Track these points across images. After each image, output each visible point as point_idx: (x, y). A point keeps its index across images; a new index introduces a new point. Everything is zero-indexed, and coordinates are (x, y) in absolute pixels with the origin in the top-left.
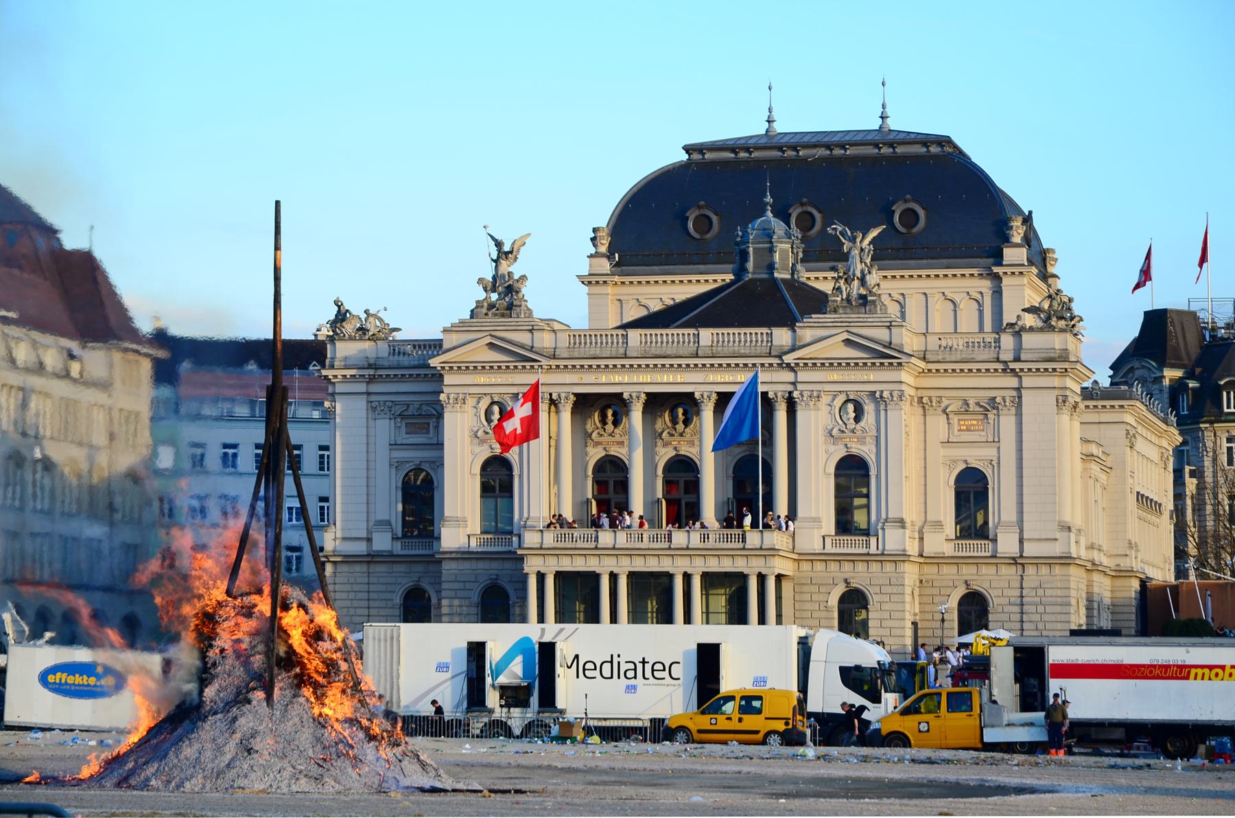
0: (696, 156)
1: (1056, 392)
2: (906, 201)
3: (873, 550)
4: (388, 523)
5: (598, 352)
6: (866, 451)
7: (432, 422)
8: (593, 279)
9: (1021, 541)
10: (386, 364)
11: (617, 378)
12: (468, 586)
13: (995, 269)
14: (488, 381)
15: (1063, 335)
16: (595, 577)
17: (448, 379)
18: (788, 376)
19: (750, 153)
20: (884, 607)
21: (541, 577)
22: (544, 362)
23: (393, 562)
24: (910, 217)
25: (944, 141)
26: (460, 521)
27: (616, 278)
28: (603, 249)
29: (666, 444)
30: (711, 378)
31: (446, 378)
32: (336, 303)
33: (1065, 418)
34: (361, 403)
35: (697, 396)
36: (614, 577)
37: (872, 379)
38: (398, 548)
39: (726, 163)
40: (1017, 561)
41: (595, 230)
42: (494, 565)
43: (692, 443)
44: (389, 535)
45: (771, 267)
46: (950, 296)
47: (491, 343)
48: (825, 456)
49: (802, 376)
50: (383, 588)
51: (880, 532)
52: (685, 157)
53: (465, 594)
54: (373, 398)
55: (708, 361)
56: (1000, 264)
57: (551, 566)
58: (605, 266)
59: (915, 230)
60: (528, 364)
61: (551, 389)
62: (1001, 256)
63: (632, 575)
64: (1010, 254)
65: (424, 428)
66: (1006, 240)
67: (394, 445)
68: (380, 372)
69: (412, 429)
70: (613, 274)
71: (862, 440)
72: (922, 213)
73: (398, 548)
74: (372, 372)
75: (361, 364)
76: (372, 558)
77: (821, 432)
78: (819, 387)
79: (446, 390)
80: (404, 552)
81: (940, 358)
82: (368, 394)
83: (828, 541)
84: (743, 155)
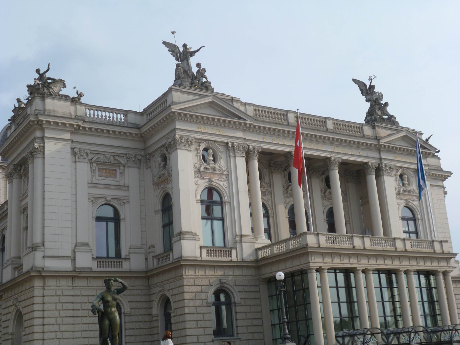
4: (86, 245)
23: (93, 277)
26: (194, 236)
32: (38, 71)
38: (94, 266)
44: (90, 254)
47: (212, 102)
49: (384, 156)
53: (203, 296)
54: (74, 145)
61: (249, 143)
67: (91, 184)
73: (94, 266)
76: (76, 275)
80: (99, 270)
82: (72, 141)
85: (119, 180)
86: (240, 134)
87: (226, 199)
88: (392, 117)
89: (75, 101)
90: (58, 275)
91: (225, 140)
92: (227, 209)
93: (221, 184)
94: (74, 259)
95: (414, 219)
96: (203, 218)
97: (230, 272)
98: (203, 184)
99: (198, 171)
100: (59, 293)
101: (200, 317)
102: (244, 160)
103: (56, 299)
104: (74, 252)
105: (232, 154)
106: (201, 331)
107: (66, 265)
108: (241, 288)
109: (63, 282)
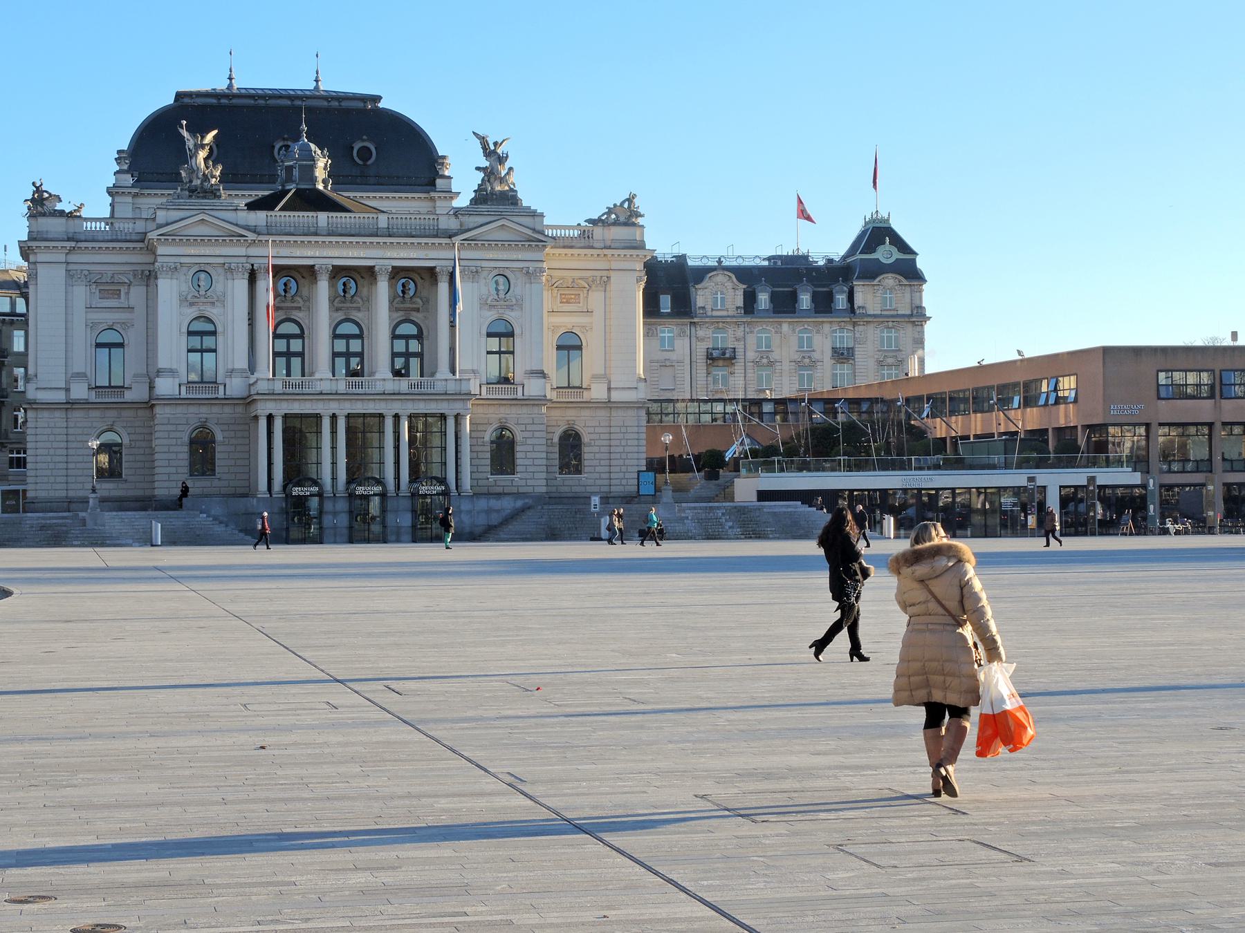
0: (187, 100)
2: (364, 141)
3: (520, 395)
4: (84, 375)
5: (292, 230)
6: (511, 316)
7: (123, 290)
8: (121, 190)
9: (609, 389)
10: (83, 238)
11: (310, 253)
12: (180, 428)
13: (433, 194)
14: (197, 253)
16: (318, 417)
17: (161, 250)
20: (529, 442)
21: (270, 418)
22: (251, 236)
25: (378, 99)
26: (172, 372)
27: (136, 190)
28: (125, 167)
29: (338, 310)
30: (389, 255)
34: (61, 271)
35: (377, 269)
36: (334, 417)
37: (520, 257)
38: (93, 397)
39: (211, 106)
40: (609, 405)
41: (119, 152)
42: (204, 409)
43: (358, 309)
45: (313, 180)
50: (80, 431)
51: (526, 382)
53: (178, 435)
54: (71, 267)
55: (389, 240)
57: (280, 409)
58: (129, 180)
59: (369, 162)
62: (434, 185)
63: (348, 416)
65: (117, 294)
68: (80, 245)
69: (104, 294)
70: (133, 186)
71: (511, 307)
74: (73, 244)
75: (60, 237)
78: (478, 264)
79: (160, 259)
83: (484, 388)
85: (123, 301)
86: (241, 251)
87: (220, 329)
88: (512, 190)
89: (70, 215)
90: (50, 406)
91: (221, 260)
92: (220, 338)
93: (212, 312)
94: (67, 390)
95: (511, 334)
96: (189, 351)
97: (215, 409)
98: (192, 312)
99: (184, 301)
100: (52, 425)
101: (173, 456)
102: (246, 282)
103: (49, 431)
104: (67, 382)
105: (229, 276)
106: (173, 470)
107: (61, 397)
108: (226, 427)
109: (57, 414)
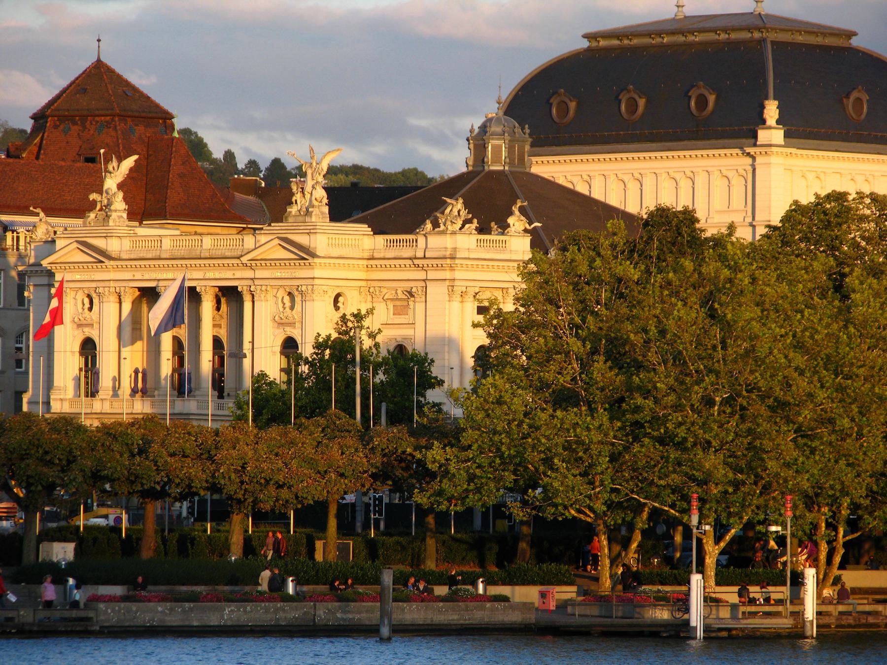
0: (594, 44)
1: (447, 283)
15: (453, 236)
18: (249, 274)
19: (631, 40)
24: (702, 102)
31: (57, 275)
33: (456, 305)
35: (198, 289)
37: (298, 275)
46: (725, 172)
48: (272, 337)
49: (259, 274)
52: (585, 44)
56: (755, 145)
60: (99, 265)
62: (755, 137)
64: (763, 136)
66: (764, 122)
72: (712, 99)
77: (269, 318)
81: (382, 255)
84: (626, 42)
